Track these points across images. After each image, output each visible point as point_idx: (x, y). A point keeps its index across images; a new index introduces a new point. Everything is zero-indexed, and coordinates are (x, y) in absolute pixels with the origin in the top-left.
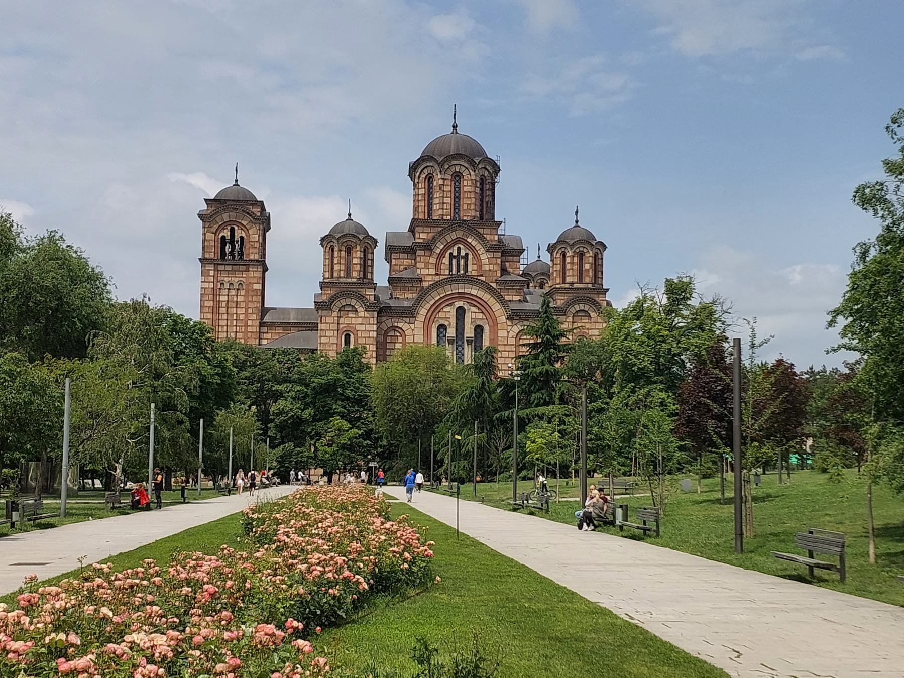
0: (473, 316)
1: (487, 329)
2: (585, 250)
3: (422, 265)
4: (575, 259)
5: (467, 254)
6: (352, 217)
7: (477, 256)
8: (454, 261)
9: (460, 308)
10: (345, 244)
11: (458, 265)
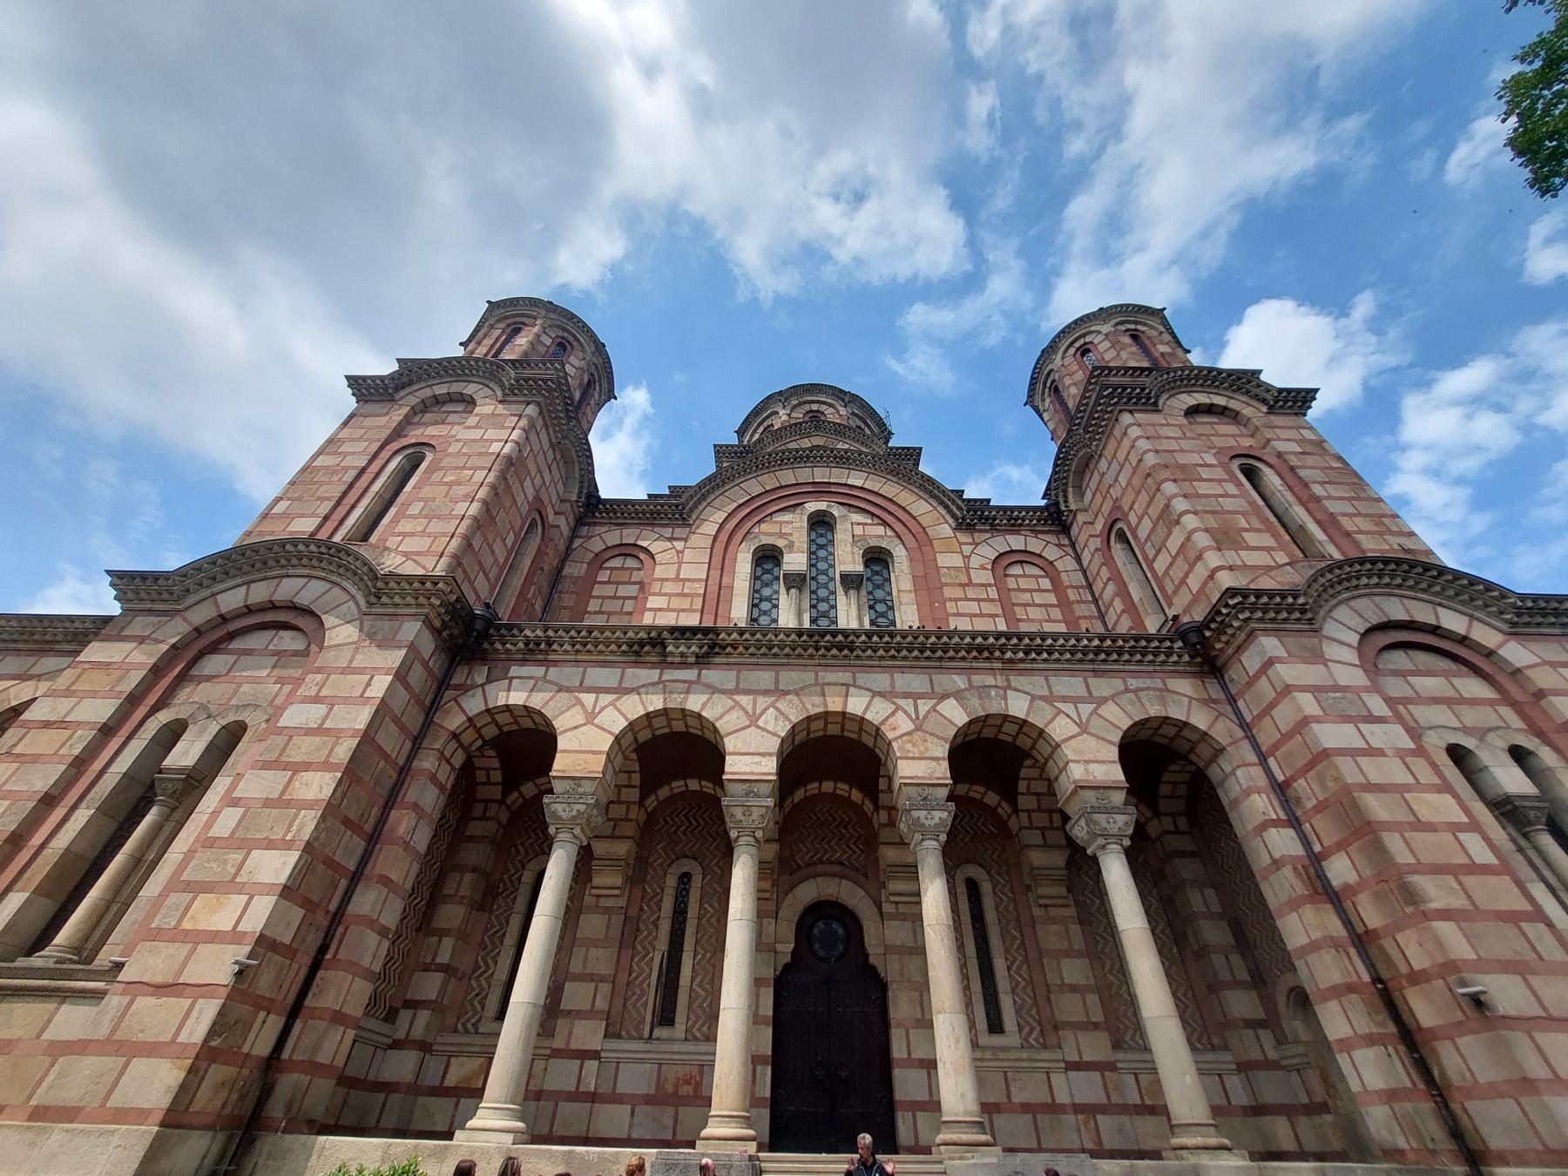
0: (858, 530)
1: (899, 553)
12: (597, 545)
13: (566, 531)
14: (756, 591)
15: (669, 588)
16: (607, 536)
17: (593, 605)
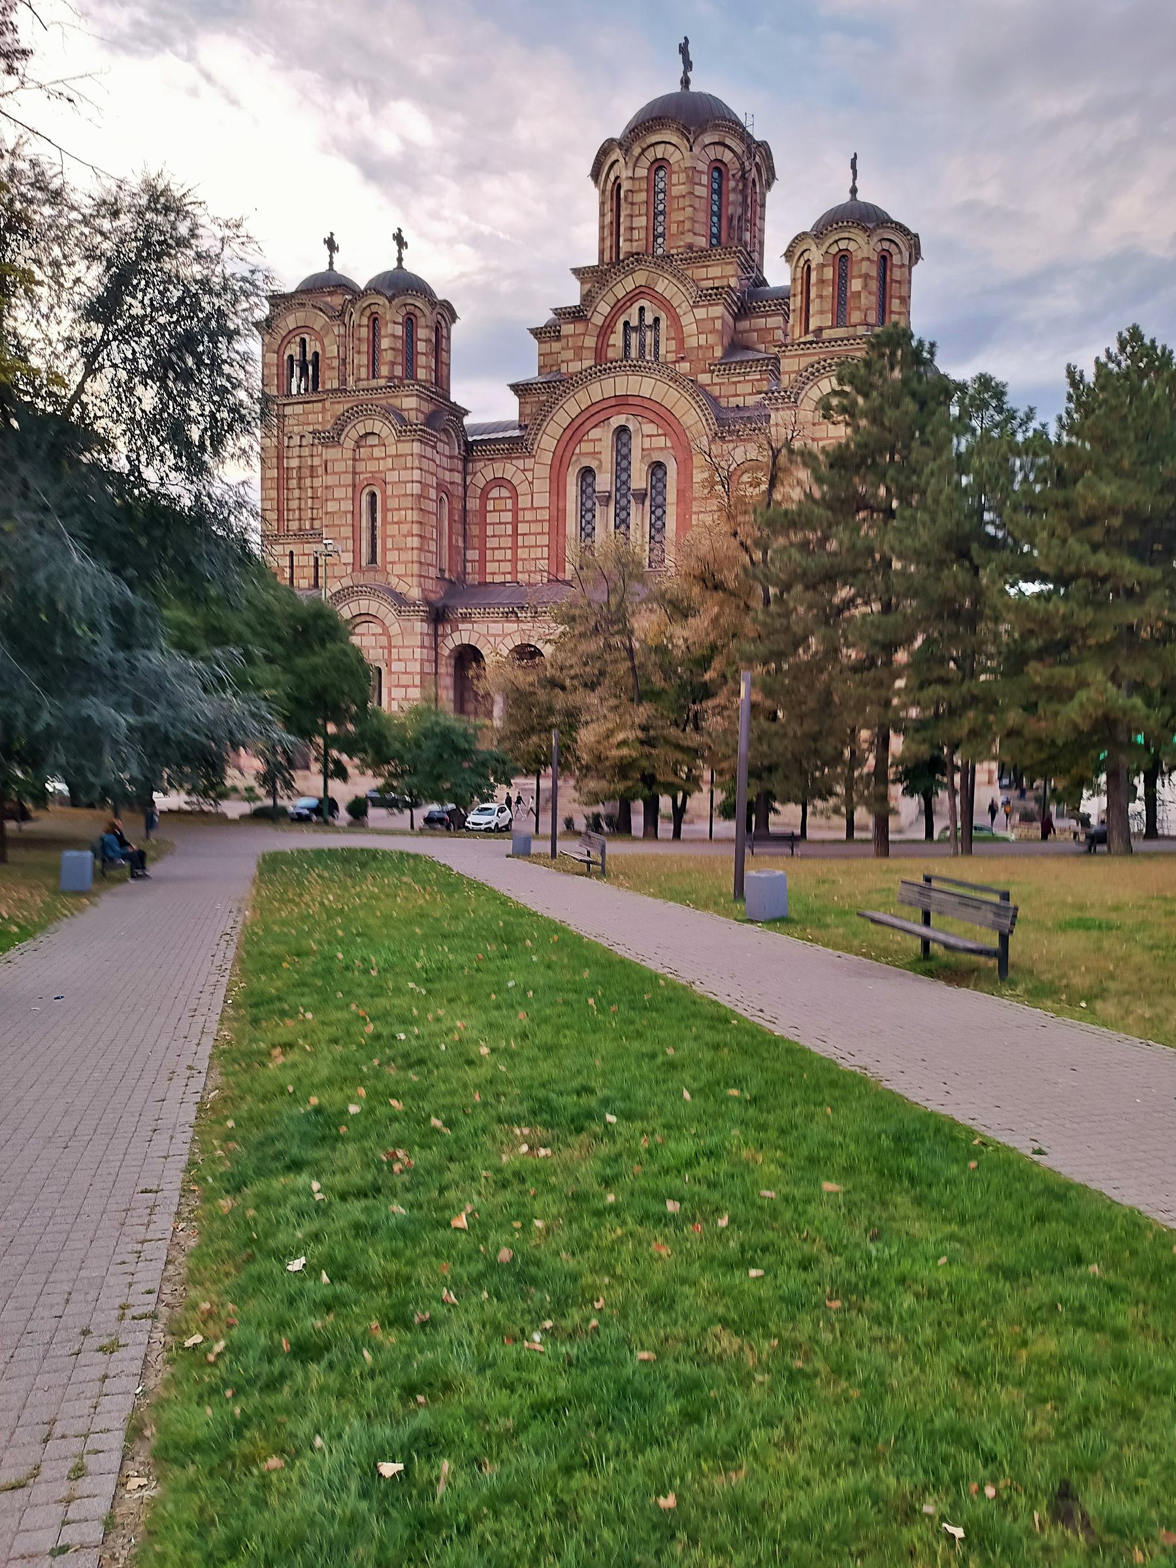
1: (672, 468)
2: (852, 247)
3: (569, 354)
4: (829, 273)
5: (657, 320)
6: (404, 264)
7: (675, 319)
8: (634, 338)
9: (622, 430)
10: (367, 313)
11: (642, 345)
12: (481, 483)
13: (458, 478)
14: (583, 504)
15: (529, 516)
16: (485, 471)
17: (489, 532)
